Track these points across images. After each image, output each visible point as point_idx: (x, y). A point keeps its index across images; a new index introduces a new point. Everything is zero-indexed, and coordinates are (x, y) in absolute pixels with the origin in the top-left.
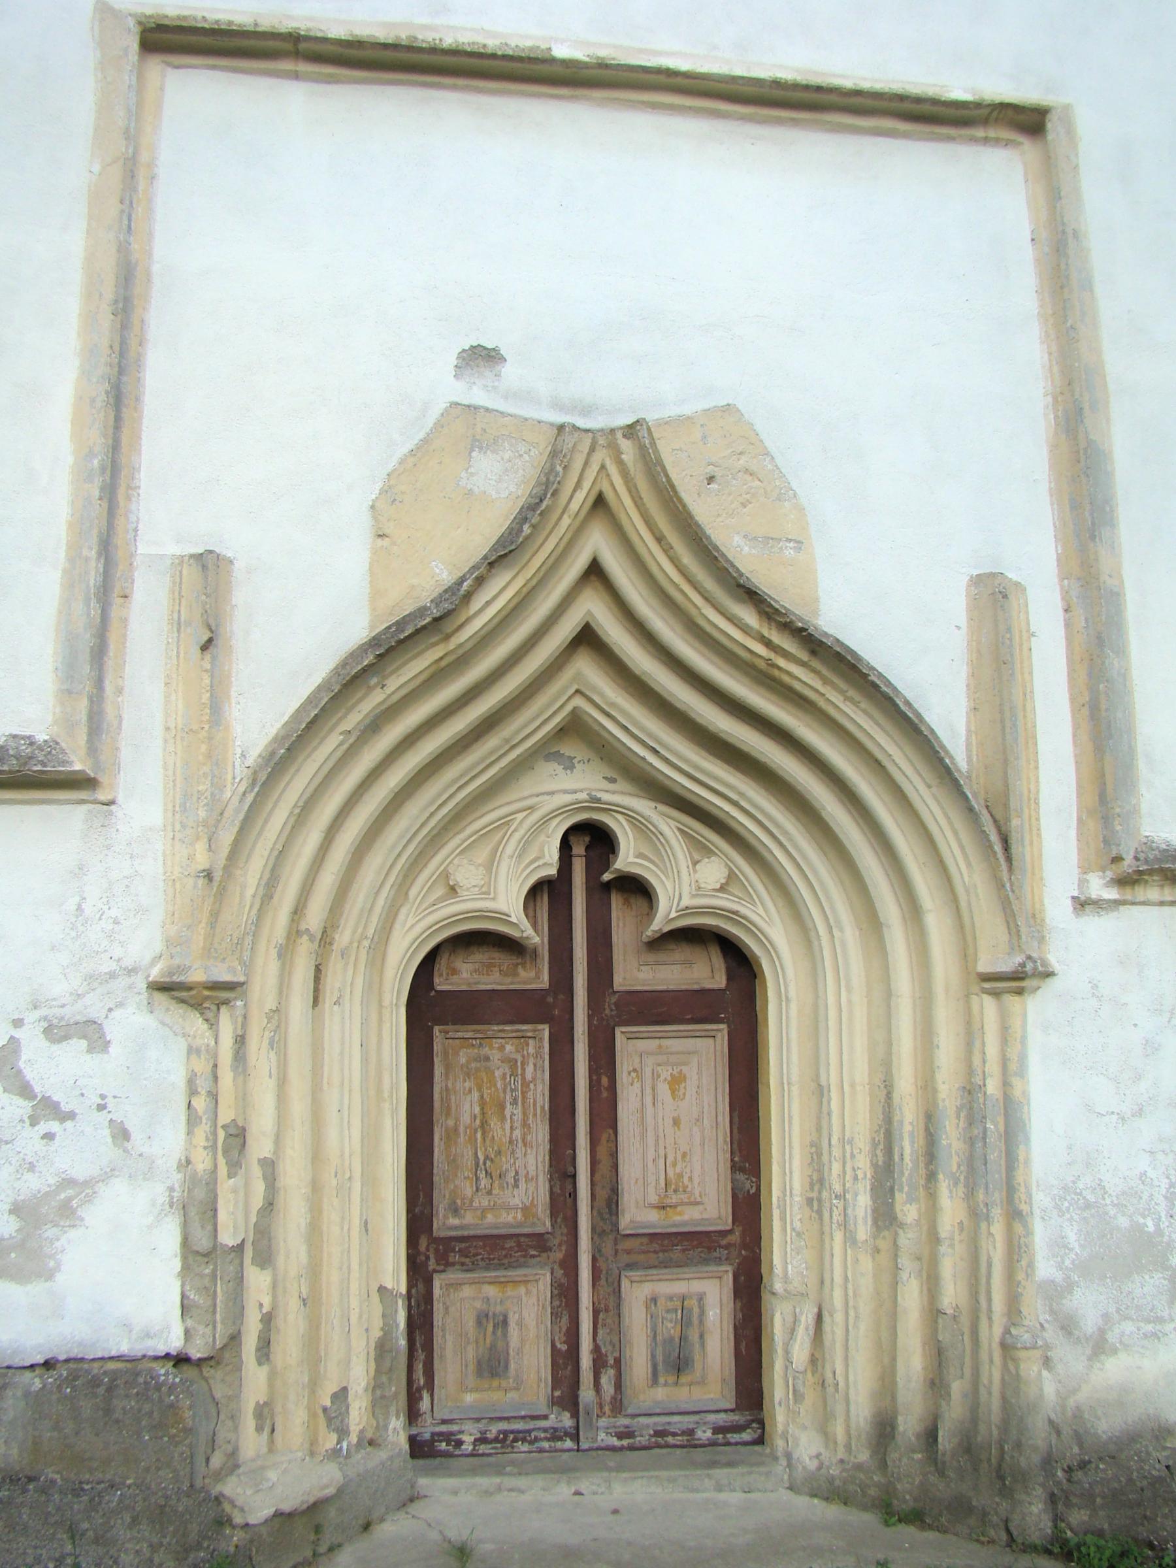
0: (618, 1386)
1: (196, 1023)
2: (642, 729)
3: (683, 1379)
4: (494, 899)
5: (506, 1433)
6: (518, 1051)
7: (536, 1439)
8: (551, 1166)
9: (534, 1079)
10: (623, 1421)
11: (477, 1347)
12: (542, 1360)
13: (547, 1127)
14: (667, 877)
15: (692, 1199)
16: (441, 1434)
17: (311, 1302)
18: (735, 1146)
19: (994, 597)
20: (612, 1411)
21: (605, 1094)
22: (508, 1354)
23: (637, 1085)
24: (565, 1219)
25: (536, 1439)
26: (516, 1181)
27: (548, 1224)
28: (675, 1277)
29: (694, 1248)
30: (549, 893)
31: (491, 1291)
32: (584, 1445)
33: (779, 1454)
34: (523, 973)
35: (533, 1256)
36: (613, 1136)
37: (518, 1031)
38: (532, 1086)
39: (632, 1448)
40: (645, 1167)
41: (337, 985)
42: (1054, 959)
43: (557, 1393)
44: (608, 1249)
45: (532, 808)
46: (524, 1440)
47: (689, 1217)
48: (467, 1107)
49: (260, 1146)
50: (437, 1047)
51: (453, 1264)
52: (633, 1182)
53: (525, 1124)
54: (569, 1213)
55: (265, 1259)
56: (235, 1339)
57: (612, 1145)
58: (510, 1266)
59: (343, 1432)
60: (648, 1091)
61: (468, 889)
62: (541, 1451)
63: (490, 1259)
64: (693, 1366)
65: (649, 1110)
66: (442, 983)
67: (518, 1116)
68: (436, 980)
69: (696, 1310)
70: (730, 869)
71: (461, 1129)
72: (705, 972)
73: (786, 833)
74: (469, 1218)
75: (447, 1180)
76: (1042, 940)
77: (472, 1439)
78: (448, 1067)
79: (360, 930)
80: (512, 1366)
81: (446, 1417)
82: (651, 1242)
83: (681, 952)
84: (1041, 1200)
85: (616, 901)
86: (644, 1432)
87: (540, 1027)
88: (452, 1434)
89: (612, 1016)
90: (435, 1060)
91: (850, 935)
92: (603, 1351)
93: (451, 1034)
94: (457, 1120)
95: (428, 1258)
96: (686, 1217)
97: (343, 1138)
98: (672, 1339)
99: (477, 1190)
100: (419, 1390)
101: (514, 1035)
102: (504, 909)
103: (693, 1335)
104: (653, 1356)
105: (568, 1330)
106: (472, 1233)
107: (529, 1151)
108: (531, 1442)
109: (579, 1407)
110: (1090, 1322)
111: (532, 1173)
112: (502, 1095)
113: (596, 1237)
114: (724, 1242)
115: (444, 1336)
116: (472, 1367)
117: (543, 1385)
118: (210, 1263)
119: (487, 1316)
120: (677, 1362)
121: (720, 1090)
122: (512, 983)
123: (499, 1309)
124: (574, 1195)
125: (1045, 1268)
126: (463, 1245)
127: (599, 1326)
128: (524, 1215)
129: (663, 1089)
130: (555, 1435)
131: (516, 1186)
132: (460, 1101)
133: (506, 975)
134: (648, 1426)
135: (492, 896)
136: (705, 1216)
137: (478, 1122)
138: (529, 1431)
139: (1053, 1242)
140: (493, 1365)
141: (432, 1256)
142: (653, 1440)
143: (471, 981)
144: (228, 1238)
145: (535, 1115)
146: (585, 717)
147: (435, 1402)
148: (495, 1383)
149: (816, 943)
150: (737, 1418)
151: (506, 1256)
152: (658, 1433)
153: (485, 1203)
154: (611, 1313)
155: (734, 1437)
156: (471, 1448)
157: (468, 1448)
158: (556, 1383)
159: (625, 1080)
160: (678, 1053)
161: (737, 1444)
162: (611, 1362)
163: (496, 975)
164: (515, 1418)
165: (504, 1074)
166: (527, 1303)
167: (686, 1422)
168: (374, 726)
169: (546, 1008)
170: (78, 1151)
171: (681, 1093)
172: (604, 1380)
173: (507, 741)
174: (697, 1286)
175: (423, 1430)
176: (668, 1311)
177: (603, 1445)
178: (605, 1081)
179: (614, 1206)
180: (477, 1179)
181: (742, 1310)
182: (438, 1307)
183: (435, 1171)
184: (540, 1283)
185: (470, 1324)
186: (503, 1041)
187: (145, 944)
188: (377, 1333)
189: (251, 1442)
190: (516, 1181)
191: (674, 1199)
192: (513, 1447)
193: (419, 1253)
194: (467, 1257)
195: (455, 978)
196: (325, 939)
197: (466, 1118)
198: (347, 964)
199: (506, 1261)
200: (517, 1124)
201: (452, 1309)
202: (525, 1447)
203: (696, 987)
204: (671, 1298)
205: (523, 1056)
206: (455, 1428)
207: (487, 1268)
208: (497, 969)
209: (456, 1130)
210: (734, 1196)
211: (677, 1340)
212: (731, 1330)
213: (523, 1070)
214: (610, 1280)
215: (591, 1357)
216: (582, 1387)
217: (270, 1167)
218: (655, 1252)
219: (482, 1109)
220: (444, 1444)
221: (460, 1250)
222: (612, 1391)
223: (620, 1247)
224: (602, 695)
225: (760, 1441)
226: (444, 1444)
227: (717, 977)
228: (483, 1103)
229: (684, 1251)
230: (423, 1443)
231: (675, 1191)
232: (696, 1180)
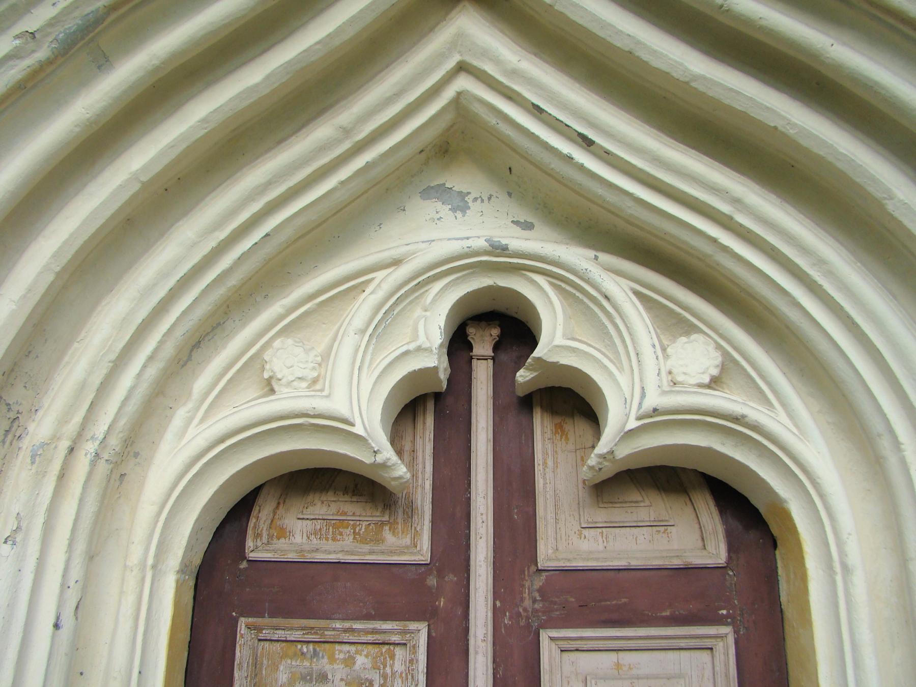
2: (564, 106)
4: (327, 397)
6: (375, 667)
14: (621, 369)
30: (431, 406)
34: (389, 538)
37: (374, 631)
41: (17, 508)
45: (396, 262)
50: (242, 653)
61: (289, 384)
66: (258, 549)
68: (250, 543)
70: (725, 354)
73: (820, 262)
79: (78, 418)
83: (651, 506)
85: (541, 425)
87: (413, 626)
89: (535, 611)
90: (236, 674)
93: (265, 634)
101: (370, 638)
102: (344, 412)
133: (364, 541)
135: (325, 393)
143: (307, 547)
146: (477, 109)
149: (892, 462)
160: (647, 677)
163: (348, 541)
169: (425, 596)
173: (347, 132)
186: (353, 648)
195: (281, 544)
198: (41, 475)
203: (677, 562)
205: (385, 676)
208: (349, 531)
224: (497, 61)
227: (711, 547)
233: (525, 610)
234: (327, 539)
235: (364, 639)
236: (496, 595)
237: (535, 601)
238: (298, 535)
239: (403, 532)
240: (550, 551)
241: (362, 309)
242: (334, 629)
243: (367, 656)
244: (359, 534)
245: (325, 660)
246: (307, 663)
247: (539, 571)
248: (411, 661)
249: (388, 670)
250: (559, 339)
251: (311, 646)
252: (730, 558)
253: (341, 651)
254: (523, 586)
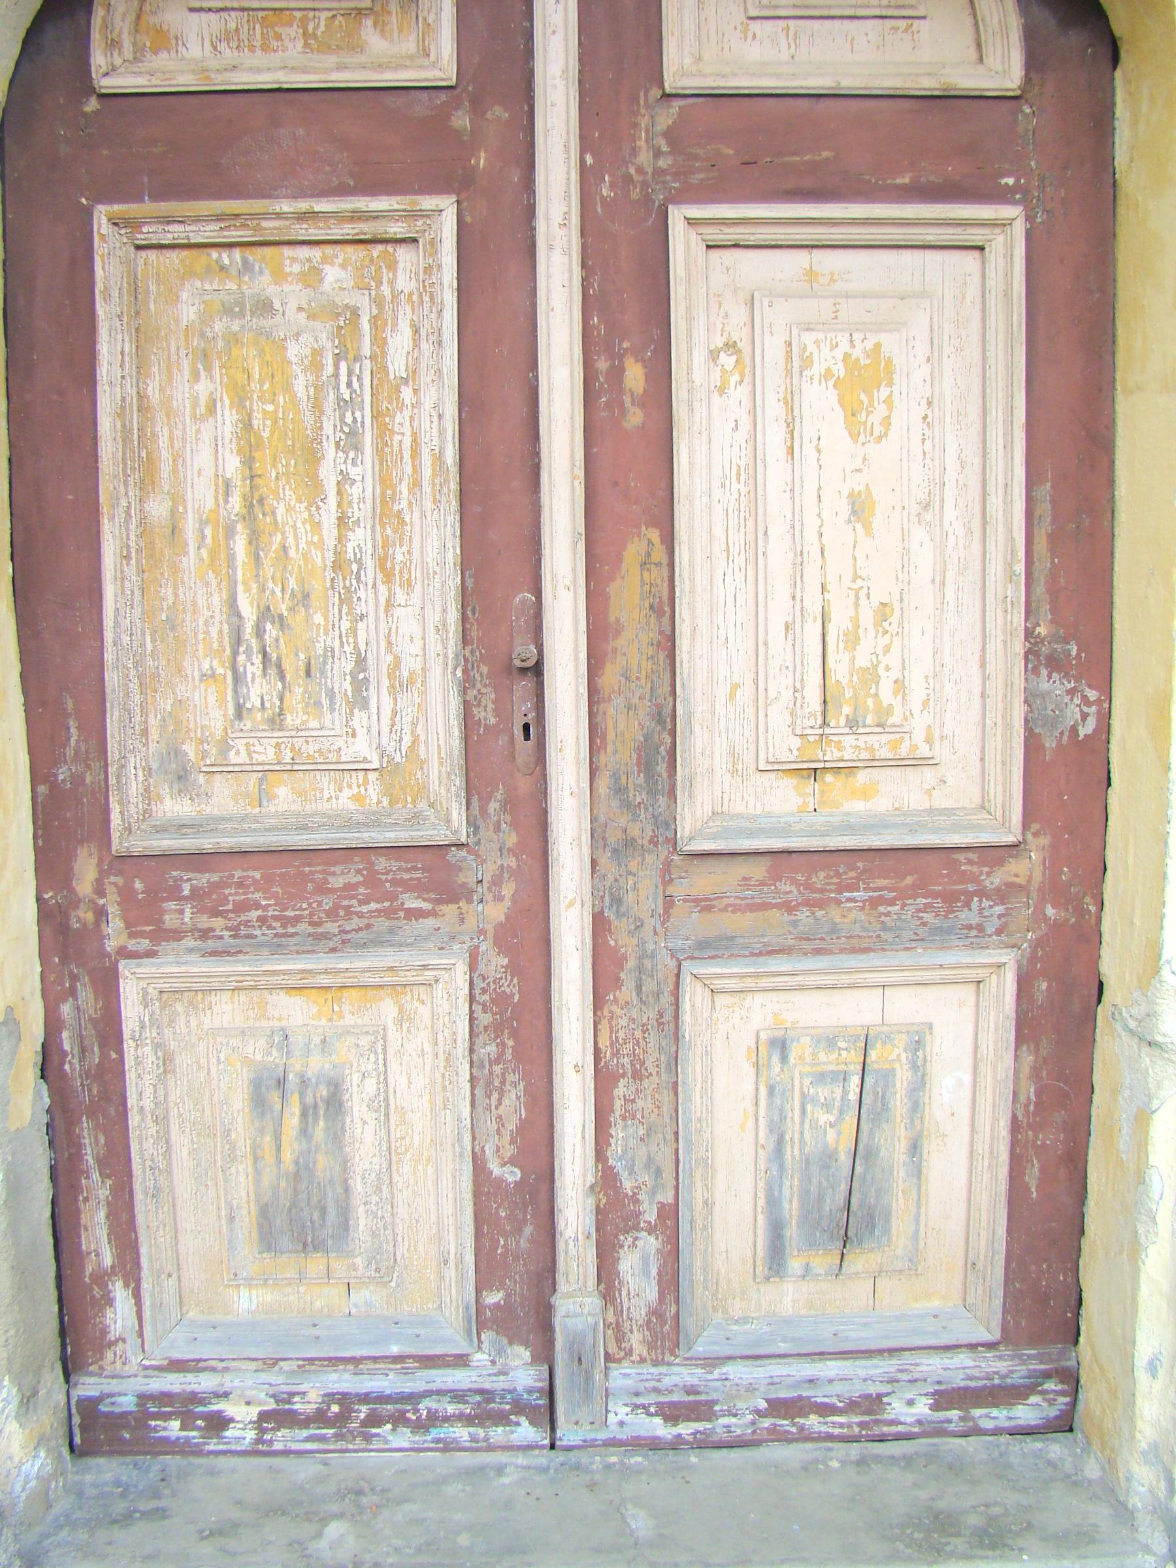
0: (670, 1279)
3: (858, 1262)
5: (345, 1399)
7: (434, 1418)
8: (465, 640)
9: (413, 374)
10: (680, 1376)
11: (258, 1172)
12: (448, 1208)
13: (452, 520)
15: (903, 751)
16: (165, 1397)
18: (1040, 589)
20: (651, 1347)
21: (635, 418)
22: (347, 1190)
23: (739, 393)
24: (509, 804)
25: (434, 1418)
26: (360, 686)
27: (458, 815)
28: (846, 979)
29: (902, 896)
31: (295, 1011)
32: (568, 1434)
33: (1135, 1502)
34: (374, 41)
35: (416, 914)
36: (659, 553)
37: (356, 216)
38: (407, 393)
39: (703, 1443)
40: (759, 649)
43: (493, 1297)
44: (643, 893)
46: (399, 1420)
47: (884, 806)
48: (203, 458)
51: (177, 935)
52: (722, 692)
53: (386, 512)
54: (524, 785)
57: (658, 576)
58: (343, 944)
60: (773, 408)
62: (448, 1446)
63: (286, 921)
64: (887, 1231)
65: (776, 473)
67: (364, 489)
68: (99, 59)
69: (903, 1076)
71: (190, 527)
74: (223, 798)
75: (149, 683)
77: (253, 1412)
78: (143, 339)
80: (362, 1221)
81: (177, 1355)
82: (775, 876)
86: (741, 1405)
87: (428, 202)
88: (195, 1398)
89: (659, 172)
90: (101, 310)
92: (628, 1185)
93: (151, 233)
94: (178, 499)
95: (101, 914)
96: (882, 804)
98: (828, 1157)
99: (240, 712)
100: (102, 1278)
101: (348, 230)
103: (892, 1144)
104: (773, 1202)
105: (523, 1128)
106: (227, 842)
107: (400, 597)
108: (420, 1426)
111: (410, 664)
112: (309, 419)
113: (605, 859)
114: (995, 880)
115: (165, 1138)
116: (247, 1223)
117: (451, 1273)
119: (281, 1083)
120: (848, 1222)
121: (996, 415)
122: (340, 67)
123: (317, 1064)
124: (534, 730)
126: (204, 879)
127: (616, 1117)
128: (388, 790)
129: (820, 403)
130: (488, 1409)
131: (359, 700)
133: (325, 48)
134: (751, 1388)
136: (941, 801)
137: (236, 502)
138: (413, 1398)
140: (303, 1220)
141: (113, 910)
142: (766, 1423)
143: (213, 64)
145: (416, 484)
147: (147, 1314)
148: (316, 1264)
150: (1002, 1366)
151: (332, 914)
152: (778, 1407)
153: (266, 753)
154: (649, 1084)
155: (998, 1416)
156: (251, 1435)
157: (241, 1434)
158: (487, 1270)
159: (698, 376)
161: (997, 1432)
162: (651, 1216)
164: (375, 1359)
165: (317, 353)
166: (398, 1048)
167: (860, 1377)
171: (876, 418)
172: (628, 1263)
174: (906, 1007)
175: (114, 1385)
176: (821, 1078)
177: (622, 1435)
178: (635, 375)
179: (662, 768)
180: (238, 678)
181: (1035, 1071)
182: (139, 1061)
183: (109, 656)
184: (439, 990)
185: (239, 1101)
186: (316, 253)
190: (360, 686)
191: (848, 748)
192: (368, 1438)
193: (74, 902)
194: (215, 913)
195: (162, 61)
197: (201, 494)
199: (332, 927)
200: (361, 511)
201: (182, 1060)
202: (403, 1438)
203: (927, 84)
204: (830, 1042)
205: (379, 302)
206: (205, 1382)
207: (278, 948)
208: (294, 31)
209: (175, 530)
210: (1032, 744)
211: (844, 1159)
212: (1004, 1132)
213: (380, 342)
214: (649, 986)
215: (591, 1201)
216: (562, 1287)
218: (788, 907)
219: (248, 462)
220: (175, 1424)
221: (196, 894)
222: (651, 1294)
223: (678, 890)
225: (1065, 1424)
226: (175, 1424)
227: (993, 59)
228: (249, 445)
229: (874, 903)
230: (119, 1420)
231: (853, 723)
232: (917, 692)
233: (640, 170)
234: (252, 48)
235: (337, 232)
236: (585, 143)
237: (658, 154)
239: (400, 31)
240: (688, 61)
242: (279, 216)
243: (343, 266)
244: (314, 36)
245: (266, 278)
246: (232, 286)
247: (667, 96)
248: (428, 270)
249: (386, 290)
251: (237, 254)
252: (1028, 79)
253: (293, 260)
254: (635, 125)
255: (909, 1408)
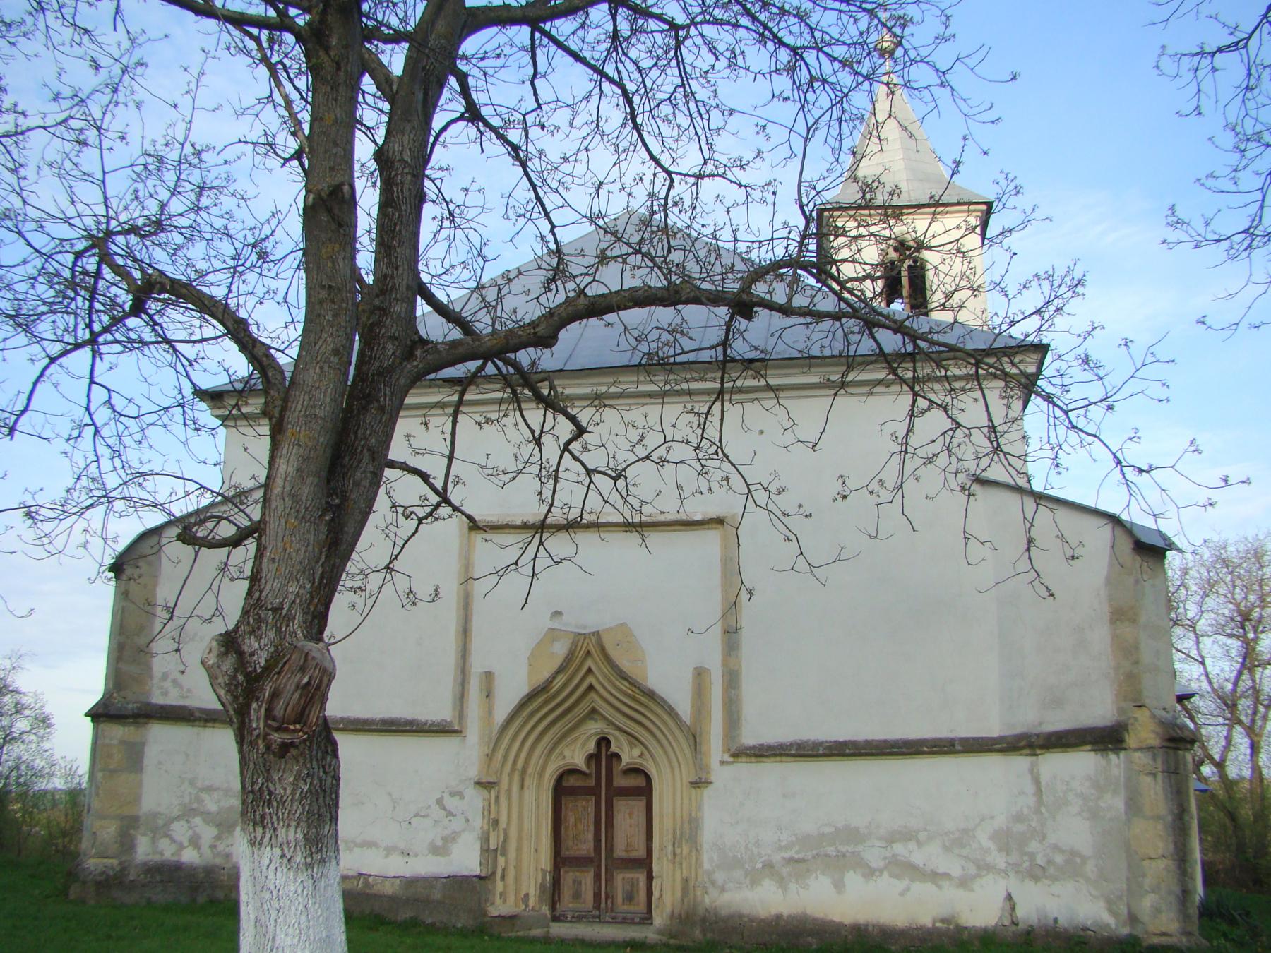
1: (485, 792)
17: (518, 868)
19: (700, 674)
30: (593, 758)
42: (713, 778)
47: (634, 854)
49: (503, 824)
55: (504, 854)
56: (494, 873)
59: (527, 906)
66: (565, 784)
72: (639, 781)
76: (708, 772)
84: (706, 846)
91: (668, 770)
97: (529, 825)
109: (601, 908)
110: (720, 882)
118: (489, 853)
120: (630, 898)
125: (706, 866)
130: (594, 917)
132: (570, 818)
139: (708, 859)
140: (577, 896)
144: (492, 847)
166: (587, 878)
168: (532, 714)
169: (593, 791)
170: (457, 824)
187: (473, 772)
188: (540, 881)
189: (498, 901)
196: (524, 770)
217: (505, 831)
238: (572, 781)
241: (580, 742)
250: (613, 748)
255: (637, 920)
